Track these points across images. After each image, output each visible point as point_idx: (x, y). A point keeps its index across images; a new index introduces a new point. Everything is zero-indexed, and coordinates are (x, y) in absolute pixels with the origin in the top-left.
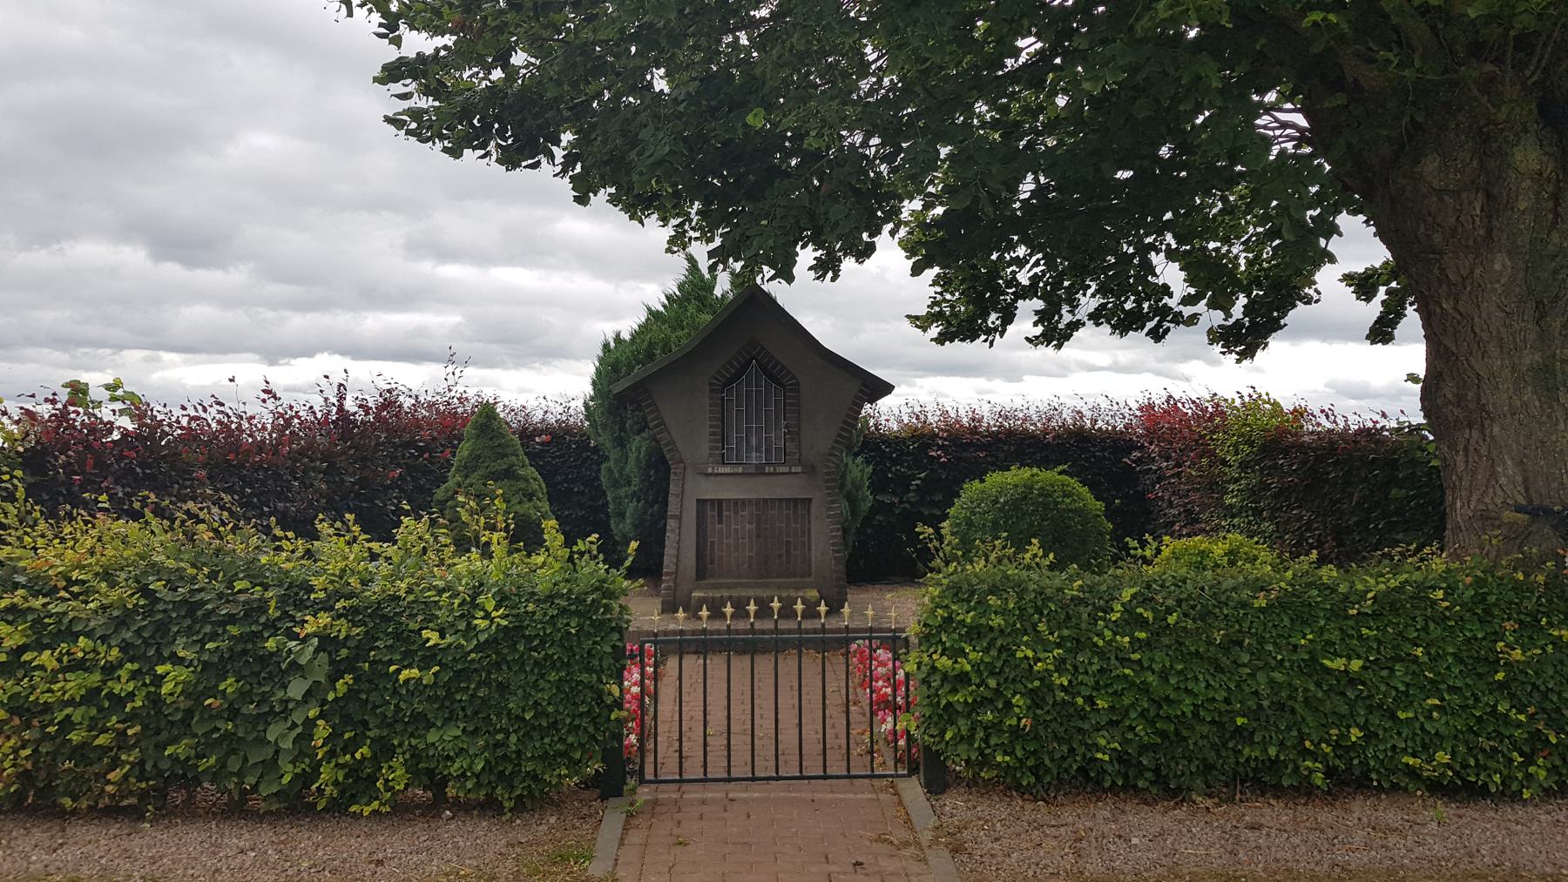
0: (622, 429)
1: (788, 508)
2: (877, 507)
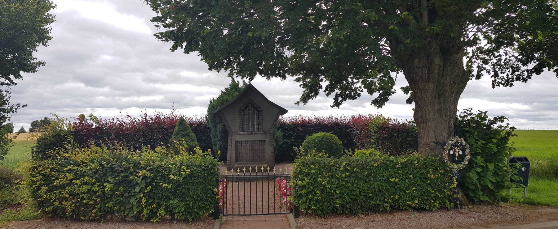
2: (284, 143)
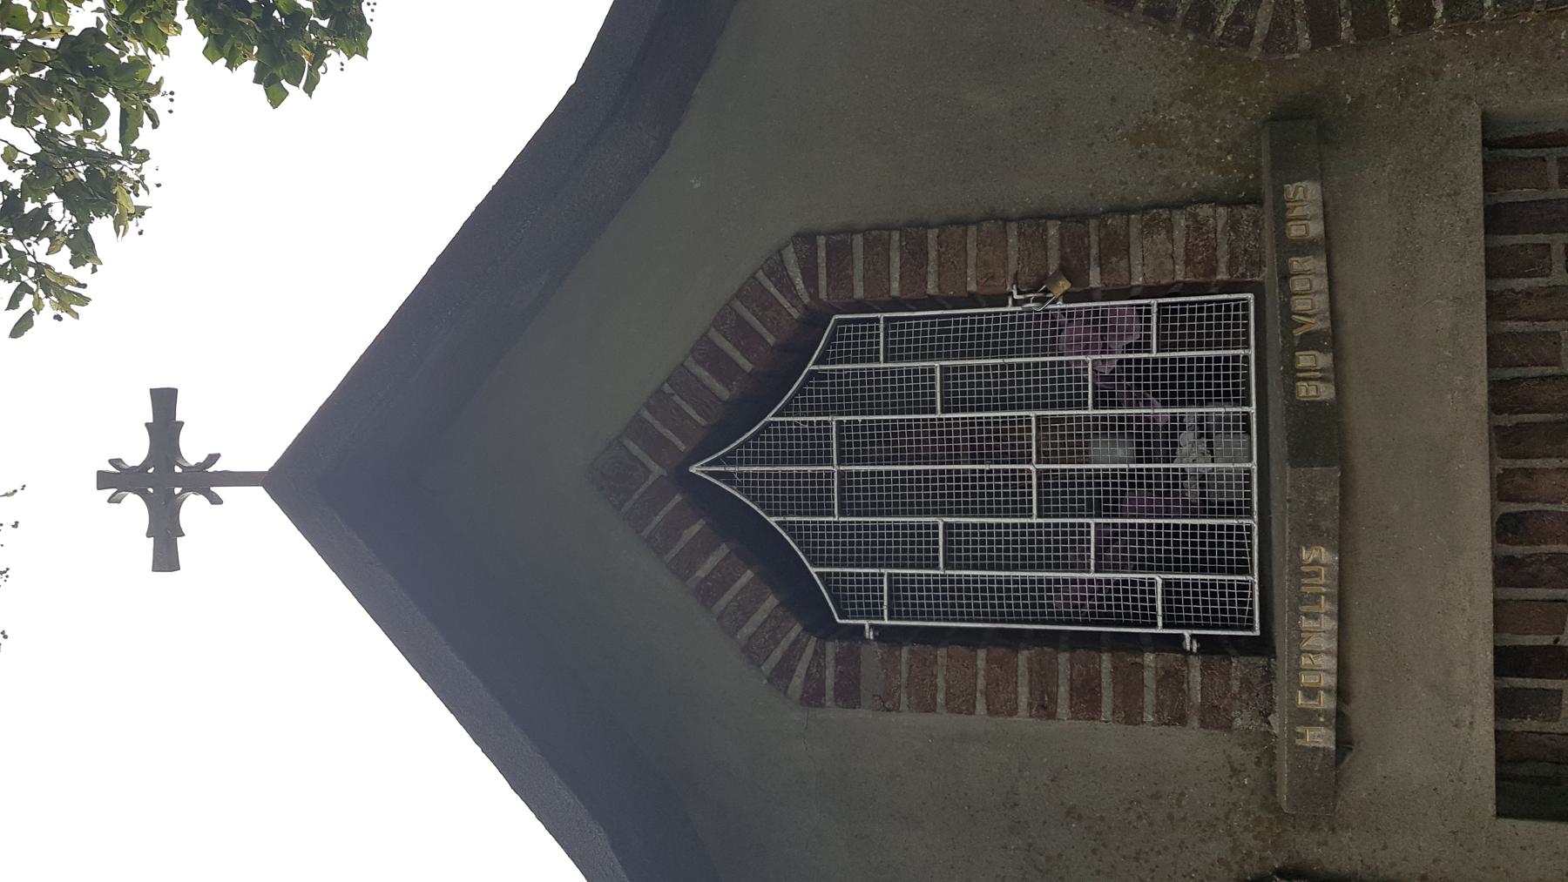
1: (1537, 262)
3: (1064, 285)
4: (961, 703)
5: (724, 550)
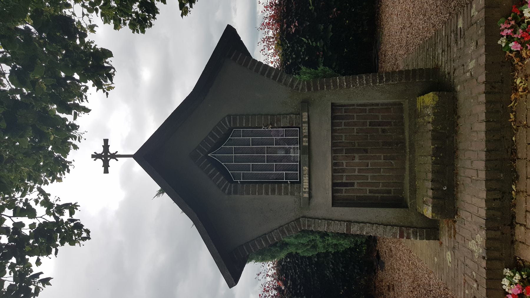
0: (275, 245)
1: (340, 124)
3: (271, 126)
4: (254, 193)
5: (214, 169)
